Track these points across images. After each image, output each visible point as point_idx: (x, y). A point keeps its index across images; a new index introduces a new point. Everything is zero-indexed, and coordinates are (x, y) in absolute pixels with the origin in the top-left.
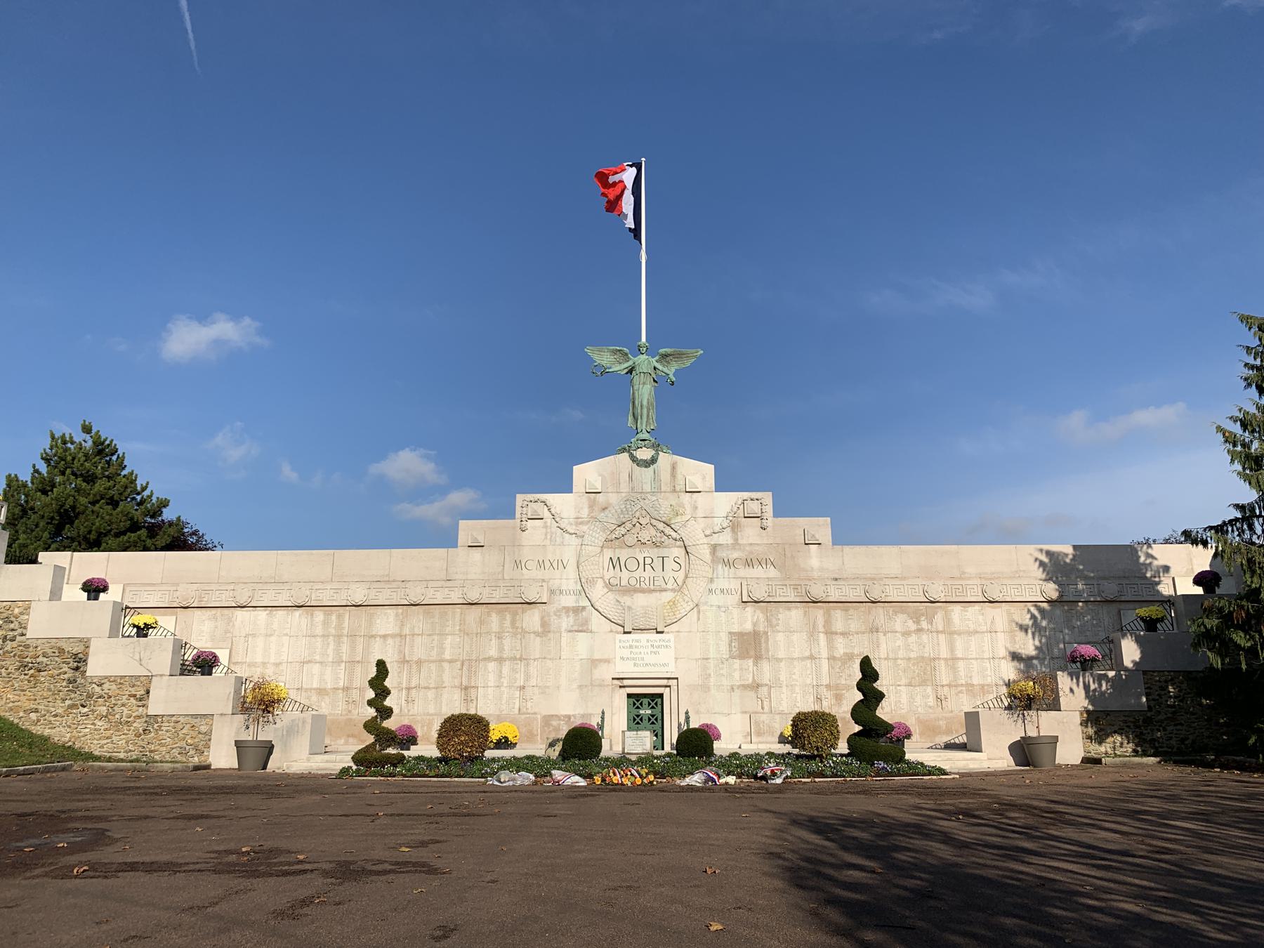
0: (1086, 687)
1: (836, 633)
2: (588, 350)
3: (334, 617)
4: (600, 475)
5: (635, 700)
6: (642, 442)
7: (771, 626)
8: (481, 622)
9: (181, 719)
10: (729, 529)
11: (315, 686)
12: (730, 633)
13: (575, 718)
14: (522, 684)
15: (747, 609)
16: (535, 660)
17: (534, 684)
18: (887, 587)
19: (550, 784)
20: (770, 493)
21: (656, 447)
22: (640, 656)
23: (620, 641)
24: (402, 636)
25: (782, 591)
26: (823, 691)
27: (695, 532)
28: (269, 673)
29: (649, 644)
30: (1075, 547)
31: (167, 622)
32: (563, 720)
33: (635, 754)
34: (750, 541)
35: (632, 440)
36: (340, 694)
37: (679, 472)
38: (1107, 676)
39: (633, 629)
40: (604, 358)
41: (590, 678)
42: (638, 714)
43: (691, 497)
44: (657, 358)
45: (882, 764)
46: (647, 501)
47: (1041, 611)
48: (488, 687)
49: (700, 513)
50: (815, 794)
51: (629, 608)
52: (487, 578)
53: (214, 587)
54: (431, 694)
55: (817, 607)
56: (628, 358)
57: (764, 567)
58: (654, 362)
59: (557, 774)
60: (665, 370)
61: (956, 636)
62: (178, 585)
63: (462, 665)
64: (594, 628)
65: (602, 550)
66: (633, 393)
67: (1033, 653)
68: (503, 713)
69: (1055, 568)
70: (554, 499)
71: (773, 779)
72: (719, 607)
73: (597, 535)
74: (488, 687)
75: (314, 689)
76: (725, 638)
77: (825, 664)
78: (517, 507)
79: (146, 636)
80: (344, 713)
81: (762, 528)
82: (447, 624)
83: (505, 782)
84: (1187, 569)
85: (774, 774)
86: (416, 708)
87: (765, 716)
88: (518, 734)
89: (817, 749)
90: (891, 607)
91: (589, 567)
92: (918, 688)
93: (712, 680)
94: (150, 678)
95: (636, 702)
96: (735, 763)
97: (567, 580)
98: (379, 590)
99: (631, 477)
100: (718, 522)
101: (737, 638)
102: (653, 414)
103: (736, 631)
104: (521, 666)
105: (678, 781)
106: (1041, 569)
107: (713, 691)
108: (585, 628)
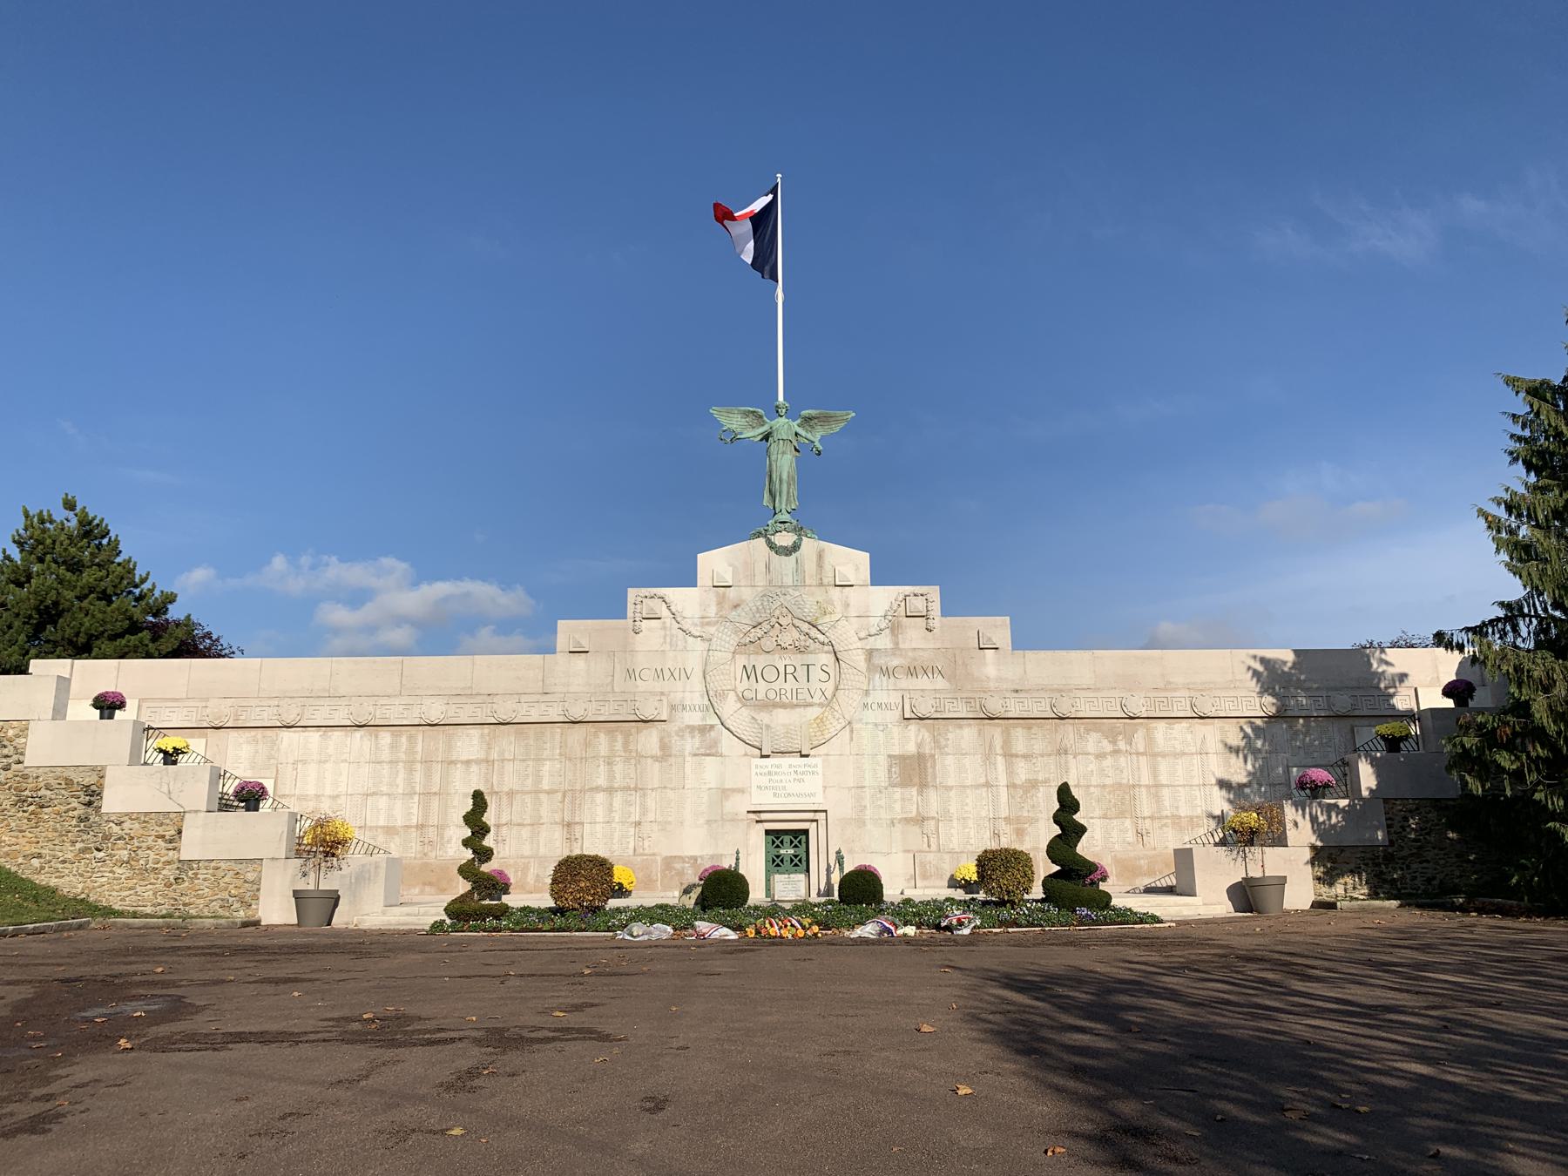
0: (1314, 819)
1: (1017, 756)
2: (714, 411)
3: (404, 739)
4: (730, 565)
5: (774, 836)
6: (782, 525)
7: (940, 748)
8: (587, 744)
9: (222, 865)
10: (887, 631)
11: (382, 823)
12: (889, 756)
13: (702, 860)
14: (637, 819)
15: (909, 728)
16: (652, 790)
17: (652, 819)
18: (1078, 700)
19: (694, 938)
20: (938, 588)
21: (799, 530)
22: (780, 785)
23: (757, 767)
24: (488, 761)
25: (952, 705)
26: (1003, 826)
27: (847, 635)
28: (326, 808)
29: (792, 770)
30: (1295, 651)
31: (197, 744)
32: (688, 863)
33: (790, 901)
34: (914, 646)
35: (770, 522)
36: (414, 833)
37: (826, 562)
38: (1338, 806)
39: (773, 752)
40: (734, 421)
41: (720, 811)
42: (777, 854)
43: (842, 592)
44: (799, 421)
45: (1085, 911)
46: (788, 597)
47: (1256, 729)
48: (595, 823)
49: (853, 612)
50: (1014, 946)
51: (768, 727)
52: (593, 691)
53: (253, 702)
54: (525, 832)
55: (995, 725)
56: (764, 421)
57: (930, 675)
58: (796, 426)
59: (702, 926)
60: (809, 436)
61: (1159, 759)
62: (207, 700)
63: (564, 796)
64: (725, 752)
65: (733, 657)
66: (770, 465)
67: (1244, 780)
68: (615, 854)
69: (1270, 678)
70: (672, 593)
71: (959, 930)
72: (876, 725)
73: (728, 639)
74: (595, 823)
75: (381, 827)
76: (883, 760)
77: (1003, 793)
78: (629, 604)
79: (175, 763)
80: (418, 856)
81: (927, 629)
82: (545, 746)
83: (638, 936)
84: (1432, 678)
85: (960, 923)
86: (507, 849)
87: (932, 855)
88: (634, 880)
89: (1008, 892)
90: (1082, 724)
91: (717, 677)
92: (1115, 821)
93: (868, 812)
94: (181, 815)
95: (775, 839)
96: (907, 911)
97: (693, 693)
98: (532, 705)
99: (768, 567)
100: (875, 623)
101: (897, 761)
102: (794, 491)
103: (897, 753)
104: (636, 797)
105: (848, 933)
106: (1255, 680)
107: (869, 826)
108: (713, 751)
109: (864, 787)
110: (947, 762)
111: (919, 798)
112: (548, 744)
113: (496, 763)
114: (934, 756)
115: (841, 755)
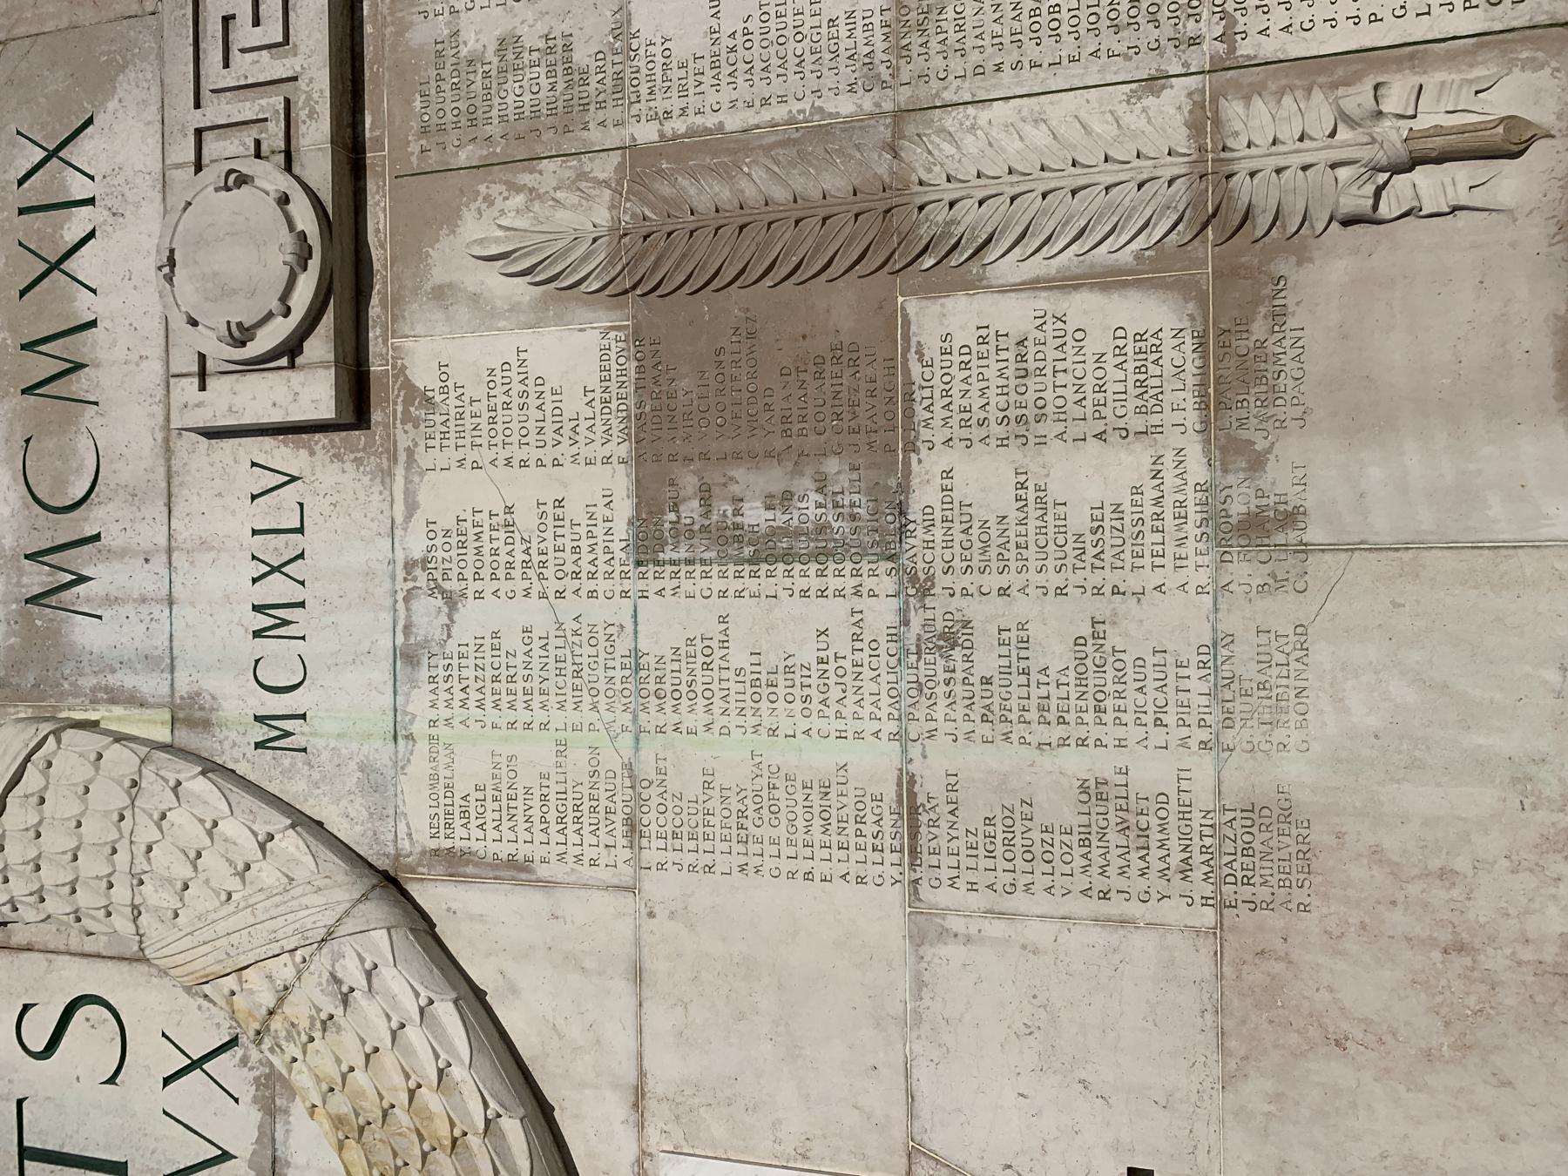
15: (423, 377)
25: (245, 34)
72: (407, 657)
103: (620, 482)
109: (908, 784)
110: (690, 42)
111: (1008, 268)
114: (631, 149)
115: (638, 974)
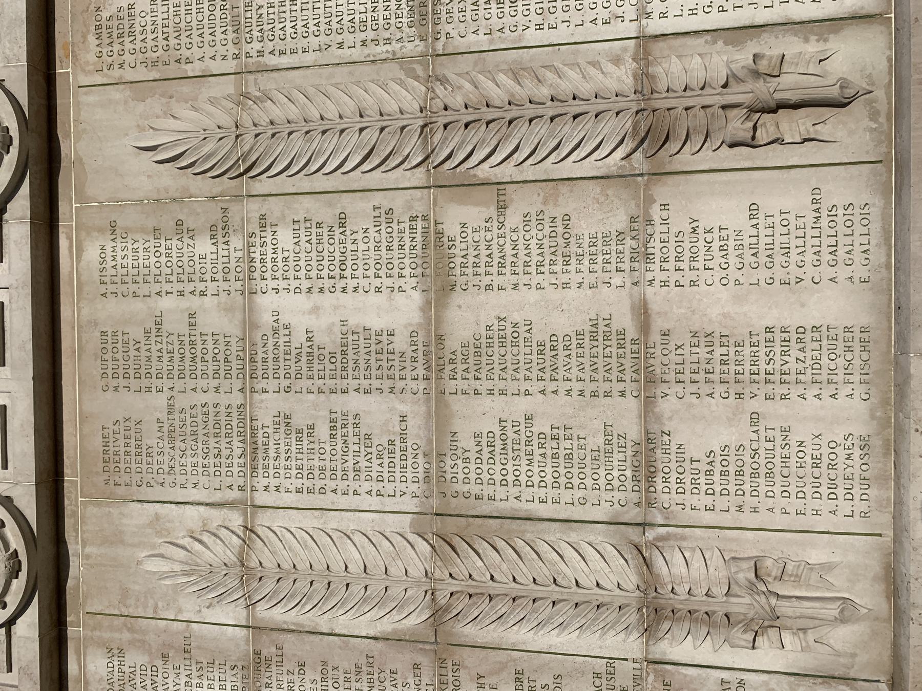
82: (175, 324)
112: (167, 303)
113: (265, 613)
